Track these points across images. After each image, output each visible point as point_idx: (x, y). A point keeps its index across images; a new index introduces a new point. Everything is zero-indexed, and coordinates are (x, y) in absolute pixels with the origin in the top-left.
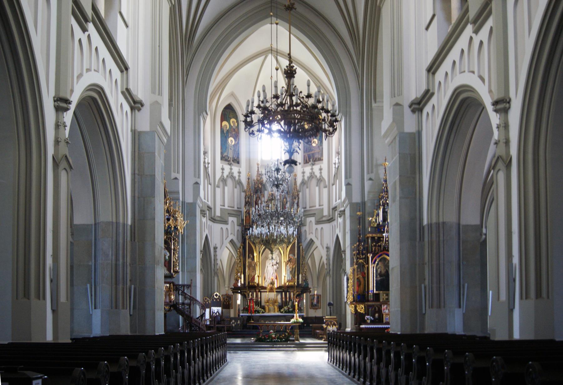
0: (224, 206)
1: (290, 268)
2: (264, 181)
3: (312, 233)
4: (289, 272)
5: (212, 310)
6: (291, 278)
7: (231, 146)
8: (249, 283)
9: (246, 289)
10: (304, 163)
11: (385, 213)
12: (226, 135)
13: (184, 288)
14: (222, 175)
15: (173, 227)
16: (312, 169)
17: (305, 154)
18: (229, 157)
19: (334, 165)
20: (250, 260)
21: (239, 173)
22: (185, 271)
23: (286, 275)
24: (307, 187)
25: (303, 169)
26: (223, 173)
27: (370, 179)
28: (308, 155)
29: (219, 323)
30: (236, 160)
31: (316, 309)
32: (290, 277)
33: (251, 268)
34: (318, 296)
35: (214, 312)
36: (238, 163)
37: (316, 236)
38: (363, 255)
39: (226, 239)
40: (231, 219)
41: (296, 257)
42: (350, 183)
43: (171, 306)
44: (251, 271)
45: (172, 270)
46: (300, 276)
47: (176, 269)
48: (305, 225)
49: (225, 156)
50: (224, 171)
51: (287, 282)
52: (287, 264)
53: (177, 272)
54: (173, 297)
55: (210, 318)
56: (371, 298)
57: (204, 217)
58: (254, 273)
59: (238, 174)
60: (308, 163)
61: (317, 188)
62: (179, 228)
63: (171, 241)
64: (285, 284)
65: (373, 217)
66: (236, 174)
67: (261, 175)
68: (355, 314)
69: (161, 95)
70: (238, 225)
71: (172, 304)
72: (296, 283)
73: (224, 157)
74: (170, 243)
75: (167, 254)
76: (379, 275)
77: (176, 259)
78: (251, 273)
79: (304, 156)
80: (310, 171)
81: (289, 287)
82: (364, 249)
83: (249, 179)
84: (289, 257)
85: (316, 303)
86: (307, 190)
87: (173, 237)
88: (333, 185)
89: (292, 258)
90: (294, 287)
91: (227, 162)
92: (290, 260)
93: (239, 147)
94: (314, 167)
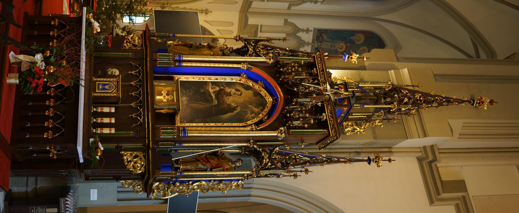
0: (261, 32)
12: (348, 38)
14: (299, 30)
18: (321, 42)
26: (303, 31)
49: (323, 36)
50: (305, 33)
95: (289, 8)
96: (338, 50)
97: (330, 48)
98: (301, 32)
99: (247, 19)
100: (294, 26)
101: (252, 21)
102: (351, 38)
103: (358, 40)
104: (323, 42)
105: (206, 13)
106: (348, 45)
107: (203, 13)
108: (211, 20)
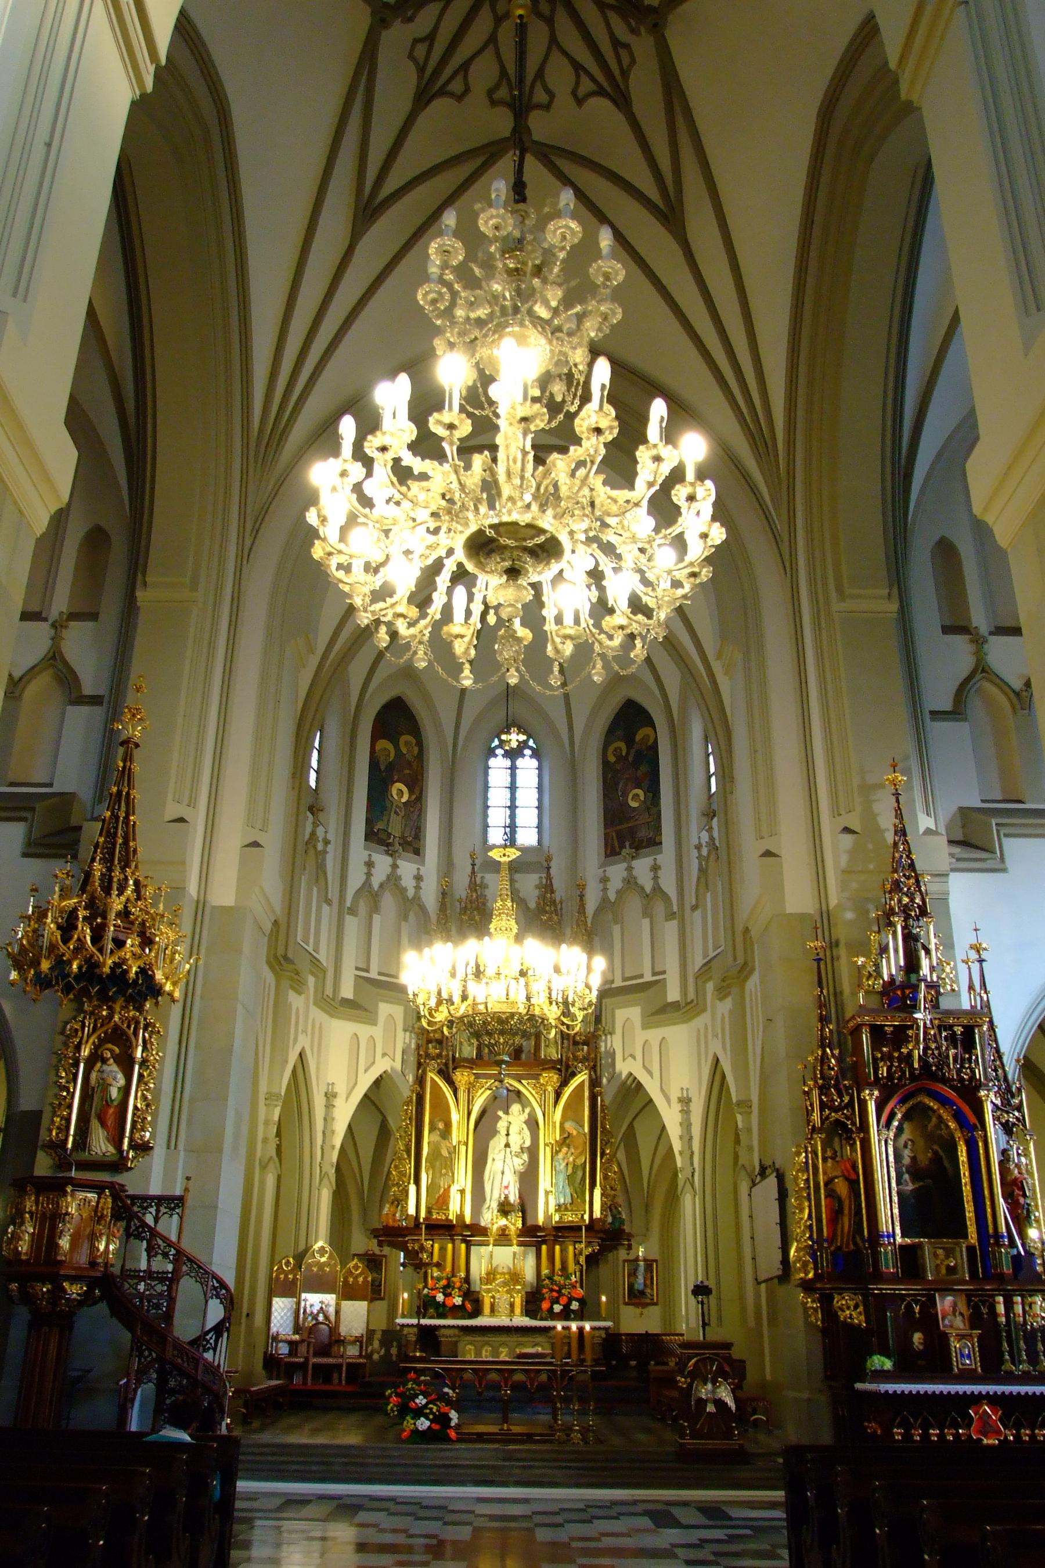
0: (367, 971)
3: (634, 1058)
4: (562, 1177)
5: (303, 1304)
6: (569, 1200)
7: (397, 806)
8: (429, 1211)
10: (607, 856)
11: (912, 944)
13: (158, 1211)
14: (367, 883)
15: (134, 969)
16: (630, 869)
19: (695, 853)
20: (436, 1137)
21: (418, 878)
22: (181, 1146)
24: (616, 923)
26: (369, 875)
27: (847, 830)
29: (324, 1350)
30: (409, 843)
31: (645, 1305)
33: (438, 1164)
34: (649, 1263)
35: (312, 1313)
36: (417, 852)
37: (644, 1066)
38: (840, 1096)
39: (366, 1071)
41: (586, 1130)
43: (93, 1283)
44: (438, 1175)
45: (126, 1141)
47: (142, 1137)
48: (611, 1034)
49: (379, 830)
50: (373, 871)
51: (556, 1211)
52: (557, 1152)
53: (143, 1148)
55: (294, 1334)
56: (889, 1266)
57: (300, 993)
58: (448, 1179)
59: (414, 883)
60: (619, 854)
62: (159, 976)
63: (136, 1034)
64: (548, 1217)
65: (867, 956)
67: (480, 886)
68: (825, 1331)
69: (25, 301)
70: (405, 1030)
71: (99, 1274)
72: (586, 1217)
73: (376, 834)
74: (133, 1038)
75: (115, 1079)
76: (908, 1172)
77: (144, 1098)
79: (606, 836)
80: (625, 874)
81: (563, 1232)
82: (843, 1073)
83: (444, 894)
85: (641, 1287)
86: (616, 929)
87: (145, 1019)
88: (694, 908)
89: (575, 1133)
92: (566, 1140)
93: (420, 810)
94: (635, 863)
95: (329, 902)
96: (404, 800)
98: (372, 878)
99: (345, 1002)
100: (358, 893)
101: (347, 991)
102: (382, 768)
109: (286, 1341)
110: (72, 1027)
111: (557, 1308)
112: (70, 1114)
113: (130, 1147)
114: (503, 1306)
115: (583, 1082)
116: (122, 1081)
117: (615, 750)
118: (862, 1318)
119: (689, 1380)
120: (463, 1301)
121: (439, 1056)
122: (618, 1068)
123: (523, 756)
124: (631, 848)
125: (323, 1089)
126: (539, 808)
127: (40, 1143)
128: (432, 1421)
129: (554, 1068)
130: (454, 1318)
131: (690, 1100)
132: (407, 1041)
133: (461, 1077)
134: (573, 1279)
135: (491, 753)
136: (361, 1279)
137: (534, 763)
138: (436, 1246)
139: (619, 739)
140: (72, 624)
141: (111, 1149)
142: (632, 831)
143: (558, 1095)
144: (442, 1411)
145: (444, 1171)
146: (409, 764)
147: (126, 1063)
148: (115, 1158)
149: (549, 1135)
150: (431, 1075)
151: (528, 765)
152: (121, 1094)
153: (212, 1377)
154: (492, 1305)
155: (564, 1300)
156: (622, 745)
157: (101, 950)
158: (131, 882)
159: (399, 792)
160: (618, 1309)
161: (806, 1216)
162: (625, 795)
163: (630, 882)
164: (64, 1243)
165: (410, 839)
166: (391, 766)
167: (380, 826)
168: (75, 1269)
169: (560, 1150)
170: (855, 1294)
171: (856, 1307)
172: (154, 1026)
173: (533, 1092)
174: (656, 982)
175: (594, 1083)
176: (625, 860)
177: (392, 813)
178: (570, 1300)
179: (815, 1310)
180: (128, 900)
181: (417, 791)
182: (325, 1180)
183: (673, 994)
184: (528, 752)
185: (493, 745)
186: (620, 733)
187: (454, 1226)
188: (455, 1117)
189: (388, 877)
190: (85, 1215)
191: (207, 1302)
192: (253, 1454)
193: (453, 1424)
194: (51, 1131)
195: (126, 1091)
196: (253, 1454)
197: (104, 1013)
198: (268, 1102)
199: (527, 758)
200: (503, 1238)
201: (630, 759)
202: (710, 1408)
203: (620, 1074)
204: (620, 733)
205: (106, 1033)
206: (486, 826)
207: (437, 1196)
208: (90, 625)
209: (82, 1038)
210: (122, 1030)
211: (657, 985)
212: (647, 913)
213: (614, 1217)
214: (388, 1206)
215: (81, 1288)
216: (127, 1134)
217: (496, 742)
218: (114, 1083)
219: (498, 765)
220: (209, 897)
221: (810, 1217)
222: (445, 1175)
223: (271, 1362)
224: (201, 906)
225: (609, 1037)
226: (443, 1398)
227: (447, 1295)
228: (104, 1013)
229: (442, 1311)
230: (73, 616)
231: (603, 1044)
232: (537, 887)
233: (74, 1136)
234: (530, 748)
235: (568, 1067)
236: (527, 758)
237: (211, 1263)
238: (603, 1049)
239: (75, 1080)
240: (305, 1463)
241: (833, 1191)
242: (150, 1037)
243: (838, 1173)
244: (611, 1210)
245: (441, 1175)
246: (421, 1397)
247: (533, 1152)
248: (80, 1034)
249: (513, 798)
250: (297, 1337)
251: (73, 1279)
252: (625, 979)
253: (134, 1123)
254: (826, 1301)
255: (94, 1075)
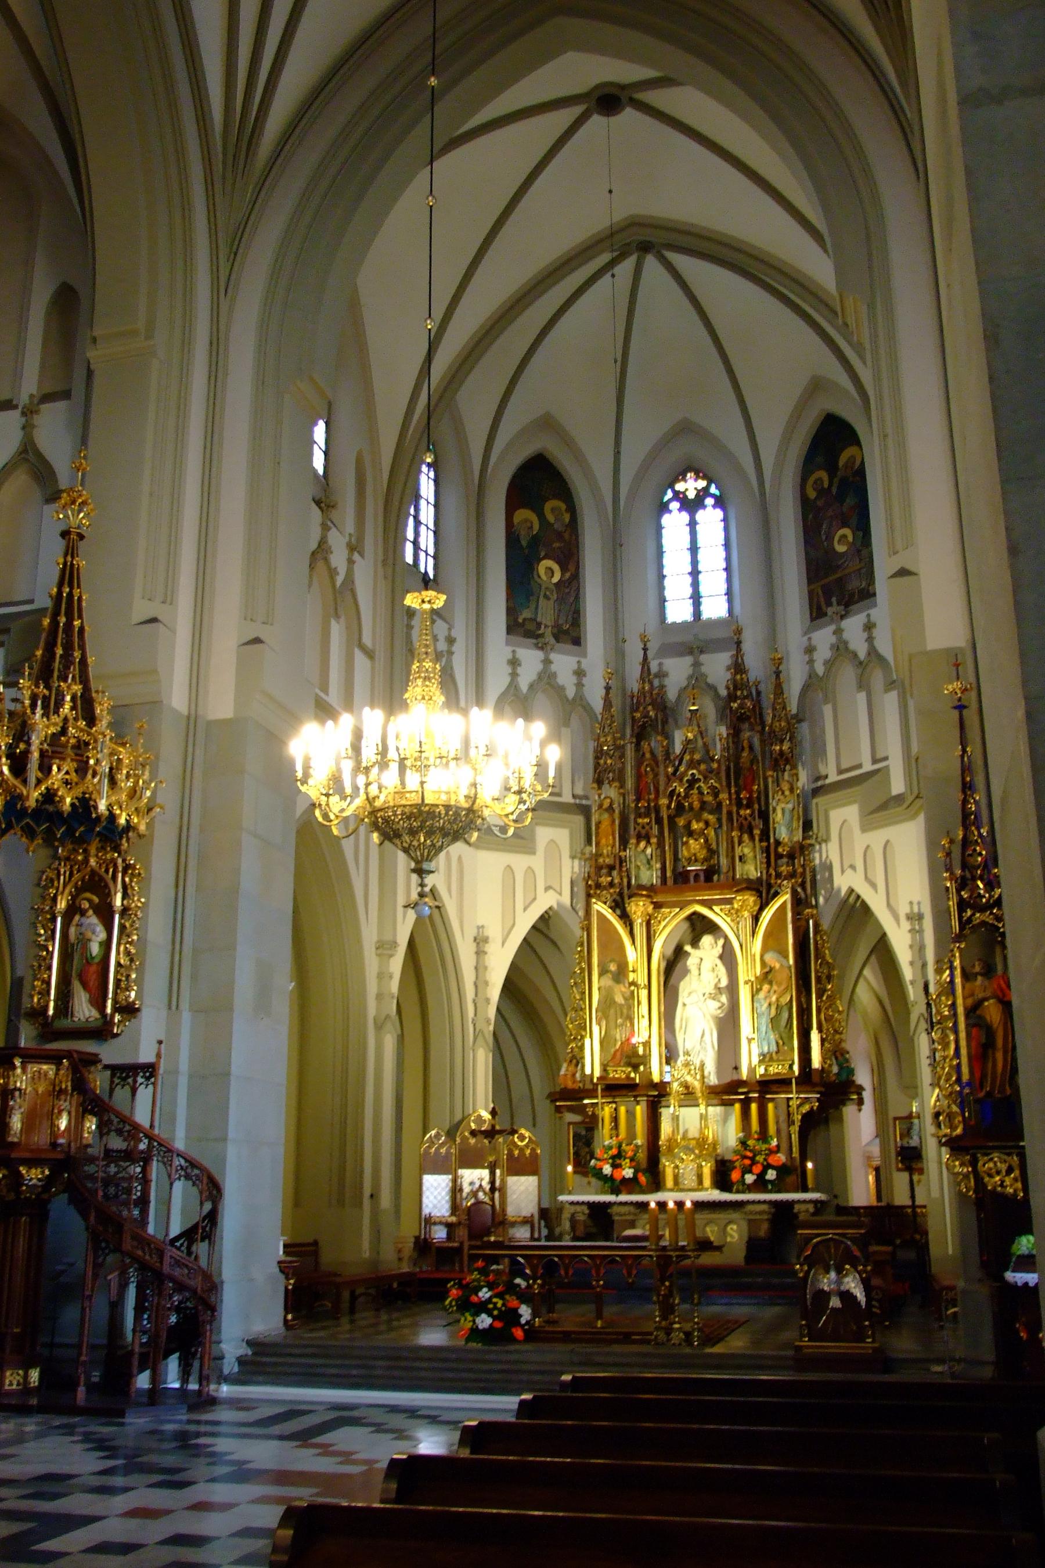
1: (770, 1005)
2: (672, 694)
3: (853, 867)
4: (764, 1020)
6: (774, 1048)
8: (604, 1068)
9: (602, 1097)
10: (812, 619)
15: (68, 800)
16: (838, 632)
17: (812, 587)
18: (539, 625)
20: (607, 981)
22: (185, 1005)
23: (755, 1036)
24: (826, 701)
25: (806, 638)
26: (514, 675)
28: (823, 587)
30: (567, 632)
32: (769, 1045)
33: (612, 1011)
36: (577, 641)
39: (525, 909)
40: (544, 835)
41: (791, 961)
42: (908, 567)
44: (612, 1024)
45: (109, 1003)
46: (815, 1037)
49: (525, 620)
50: (519, 670)
51: (760, 1062)
52: (759, 990)
53: (129, 1010)
54: (63, 1123)
59: (574, 680)
60: (826, 614)
61: (862, 697)
63: (114, 878)
64: (752, 1070)
66: (566, 679)
67: (656, 676)
70: (573, 857)
72: (796, 1068)
75: (94, 932)
77: (128, 953)
78: (612, 1032)
79: (811, 593)
80: (833, 639)
81: (767, 1086)
84: (763, 963)
86: (827, 710)
87: (124, 861)
89: (777, 966)
90: (791, 1083)
91: (534, 641)
92: (767, 976)
93: (578, 589)
94: (845, 624)
97: (552, 602)
98: (519, 679)
102: (524, 543)
103: (529, 525)
104: (539, 620)
105: (486, 940)
106: (543, 554)
107: (486, 949)
108: (500, 929)
109: (441, 1223)
110: (47, 877)
111: (750, 1178)
112: (50, 977)
113: (115, 1009)
114: (689, 1180)
115: (785, 902)
116: (103, 935)
117: (815, 482)
118: (1019, 1185)
119: (806, 1268)
120: (635, 1173)
121: (611, 884)
122: (836, 885)
123: (704, 507)
124: (839, 604)
125: (471, 933)
126: (727, 569)
127: (23, 1011)
128: (495, 1318)
129: (748, 888)
130: (630, 1193)
131: (920, 917)
132: (576, 869)
133: (638, 908)
134: (774, 1142)
135: (664, 508)
136: (528, 1152)
137: (719, 514)
138: (622, 1110)
139: (820, 468)
140: (43, 407)
141: (95, 1014)
142: (841, 582)
143: (756, 919)
144: (510, 1305)
145: (619, 1021)
146: (560, 536)
147: (105, 914)
148: (100, 1023)
149: (747, 971)
150: (600, 907)
151: (710, 518)
152: (103, 948)
153: (186, 1271)
154: (676, 1177)
155: (757, 1169)
156: (823, 475)
157: (25, 782)
158: (68, 698)
159: (550, 573)
160: (891, 1174)
161: (952, 1052)
162: (830, 538)
163: (841, 648)
164: (16, 1122)
165: (566, 627)
166: (535, 541)
167: (526, 614)
168: (32, 1151)
169: (761, 989)
170: (1009, 1154)
171: (1009, 1170)
172: (134, 868)
173: (728, 919)
174: (877, 771)
175: (799, 903)
176: (832, 621)
177: (541, 598)
178: (767, 1167)
179: (966, 1176)
180: (66, 720)
181: (572, 567)
182: (480, 1039)
183: (898, 785)
184: (709, 501)
185: (666, 499)
186: (820, 459)
187: (637, 1085)
188: (633, 955)
189: (540, 677)
190: (40, 1090)
191: (171, 1184)
192: (291, 1355)
193: (523, 1321)
194: (32, 997)
195: (107, 945)
196: (291, 1355)
197: (80, 858)
198: (379, 951)
199: (709, 509)
200: (688, 1097)
201: (834, 490)
202: (835, 1302)
203: (839, 890)
204: (820, 459)
205: (83, 880)
206: (662, 600)
207: (613, 1050)
208: (61, 405)
209: (57, 889)
210: (100, 876)
211: (879, 775)
212: (863, 684)
213: (841, 1068)
214: (565, 1066)
215: (43, 1172)
216: (110, 996)
217: (669, 494)
218: (94, 937)
219: (674, 522)
220: (200, 712)
221: (957, 1053)
222: (622, 1025)
223: (423, 1246)
224: (192, 722)
225: (824, 845)
226: (512, 1288)
227: (615, 1166)
228: (80, 858)
229: (617, 1186)
230: (47, 398)
231: (817, 855)
232: (728, 668)
233: (55, 1001)
234: (713, 496)
235: (769, 886)
236: (709, 509)
237: (173, 1140)
238: (817, 862)
239: (53, 938)
240: (341, 1366)
241: (981, 1018)
242: (131, 881)
243: (988, 994)
244: (836, 1058)
245: (616, 1026)
246: (485, 1290)
247: (732, 989)
248: (56, 883)
249: (695, 562)
250: (454, 1219)
251: (31, 1163)
252: (840, 772)
253: (118, 982)
254: (974, 1163)
255: (72, 930)
